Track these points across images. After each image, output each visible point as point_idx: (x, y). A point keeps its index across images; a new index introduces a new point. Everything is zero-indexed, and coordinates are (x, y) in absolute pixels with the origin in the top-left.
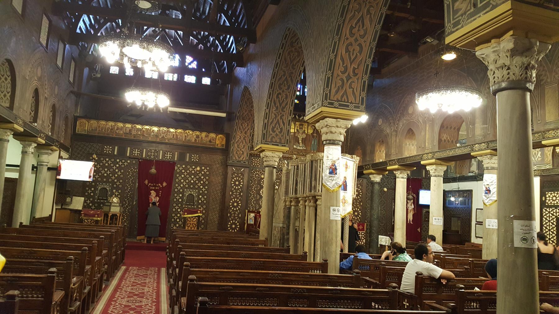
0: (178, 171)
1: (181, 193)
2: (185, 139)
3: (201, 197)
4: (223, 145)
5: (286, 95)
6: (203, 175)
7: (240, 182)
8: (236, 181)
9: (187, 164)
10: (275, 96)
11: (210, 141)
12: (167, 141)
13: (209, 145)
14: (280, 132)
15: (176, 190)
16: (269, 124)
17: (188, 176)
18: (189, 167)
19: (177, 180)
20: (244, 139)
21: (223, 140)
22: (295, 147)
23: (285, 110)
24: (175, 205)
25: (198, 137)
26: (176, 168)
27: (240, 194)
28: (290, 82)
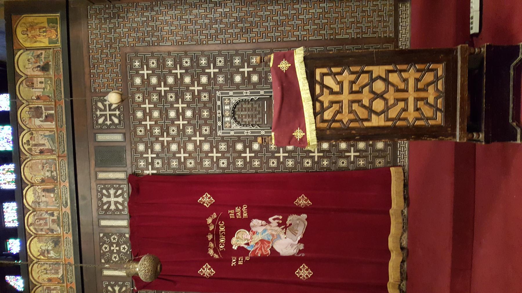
0: (158, 164)
1: (231, 146)
2: (51, 151)
3: (238, 79)
6: (162, 79)
9: (132, 138)
11: (45, 68)
12: (68, 210)
13: (57, 69)
15: (223, 163)
17: (173, 131)
18: (140, 132)
19: (191, 164)
24: (273, 163)
25: (37, 112)
26: (150, 171)
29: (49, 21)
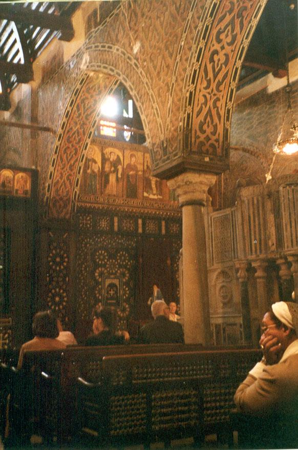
4: (26, 192)
5: (227, 55)
7: (62, 257)
8: (55, 256)
10: (208, 55)
14: (214, 133)
16: (195, 116)
20: (68, 179)
21: (26, 182)
22: (145, 194)
23: (222, 88)
27: (64, 280)
28: (237, 29)
29: (27, 191)
